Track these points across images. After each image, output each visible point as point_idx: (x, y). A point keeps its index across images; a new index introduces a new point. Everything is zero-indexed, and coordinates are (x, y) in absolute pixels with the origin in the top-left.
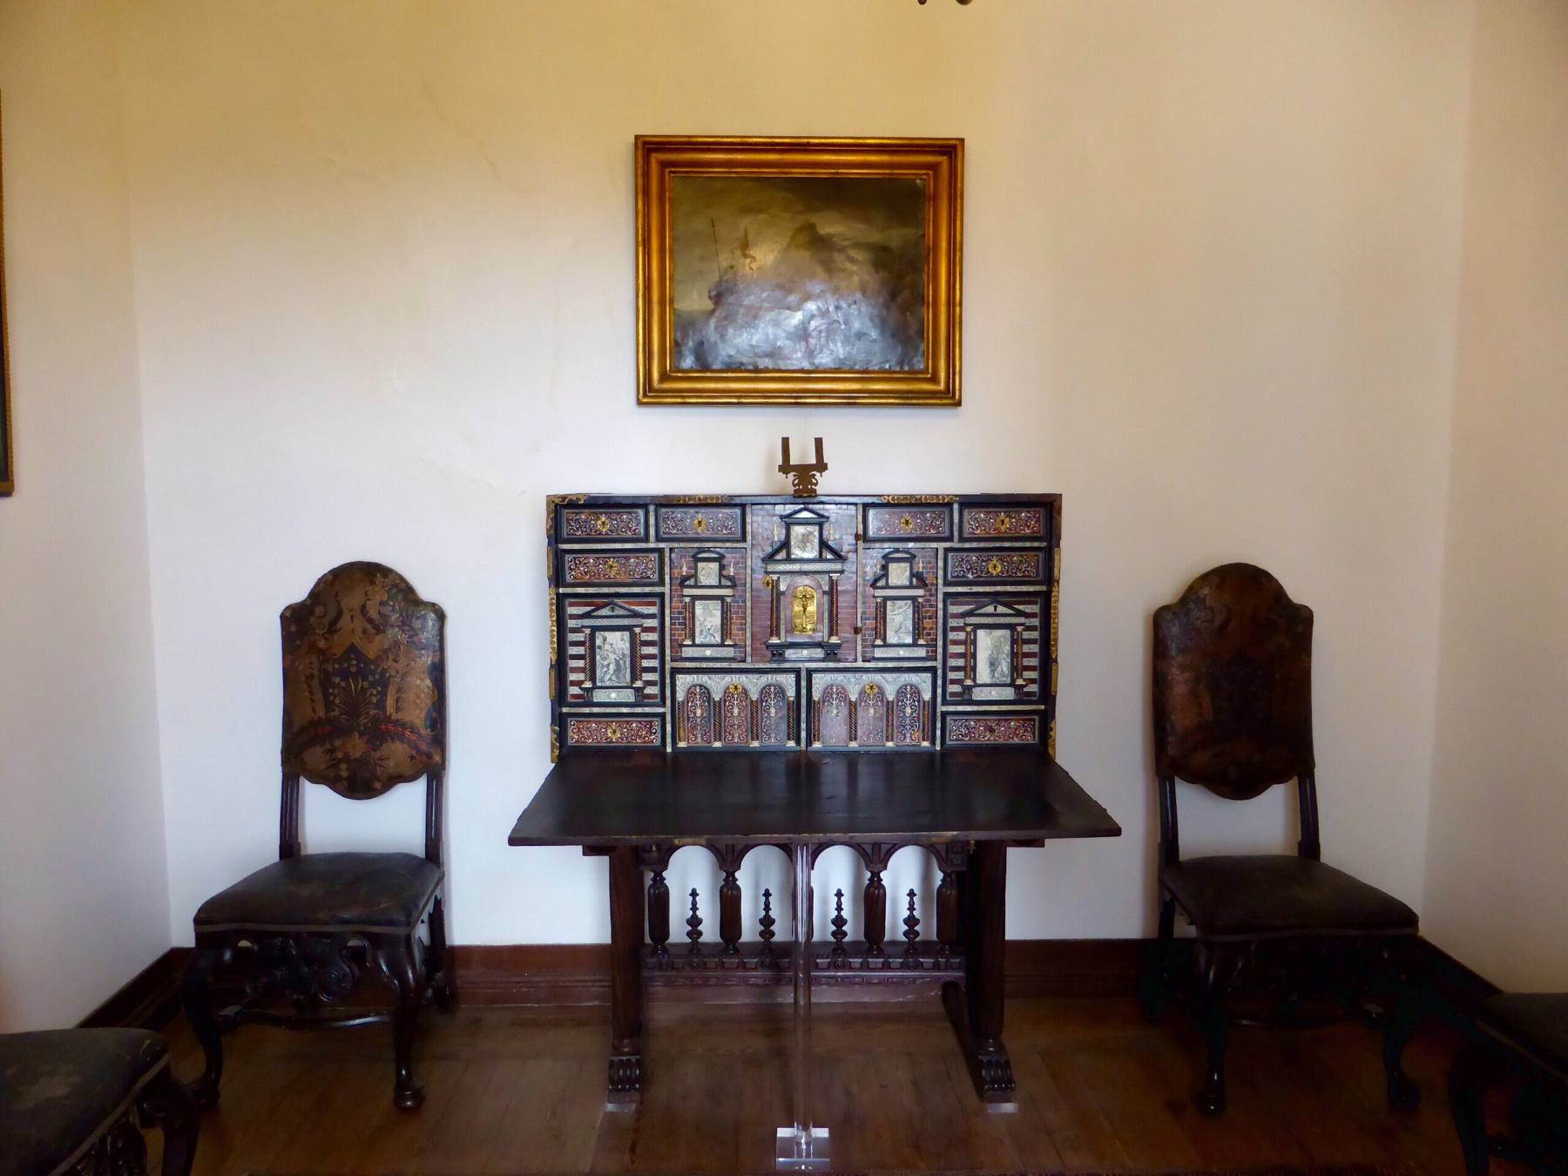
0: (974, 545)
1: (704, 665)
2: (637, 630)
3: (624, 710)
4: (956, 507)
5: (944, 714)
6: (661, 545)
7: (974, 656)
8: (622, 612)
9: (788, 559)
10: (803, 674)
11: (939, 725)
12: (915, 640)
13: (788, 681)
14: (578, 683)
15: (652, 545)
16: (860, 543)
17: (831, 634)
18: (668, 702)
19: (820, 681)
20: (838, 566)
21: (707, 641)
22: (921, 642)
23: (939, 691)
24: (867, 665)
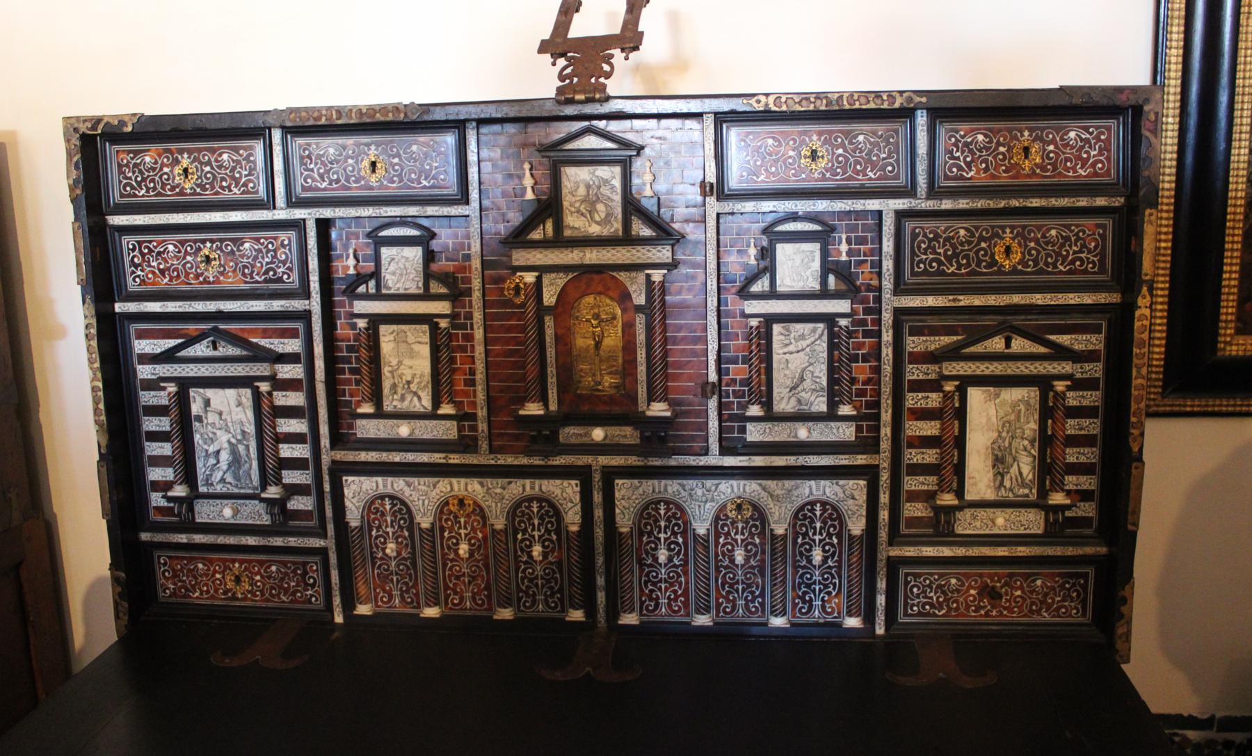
0: (963, 204)
1: (397, 457)
2: (264, 387)
3: (251, 541)
4: (921, 119)
5: (894, 565)
6: (299, 214)
7: (960, 442)
8: (232, 351)
9: (559, 241)
10: (597, 477)
11: (882, 584)
12: (833, 404)
13: (566, 492)
14: (165, 486)
15: (281, 214)
16: (711, 200)
17: (651, 398)
18: (330, 527)
19: (629, 496)
20: (663, 254)
21: (404, 406)
22: (845, 410)
23: (884, 515)
24: (730, 461)
